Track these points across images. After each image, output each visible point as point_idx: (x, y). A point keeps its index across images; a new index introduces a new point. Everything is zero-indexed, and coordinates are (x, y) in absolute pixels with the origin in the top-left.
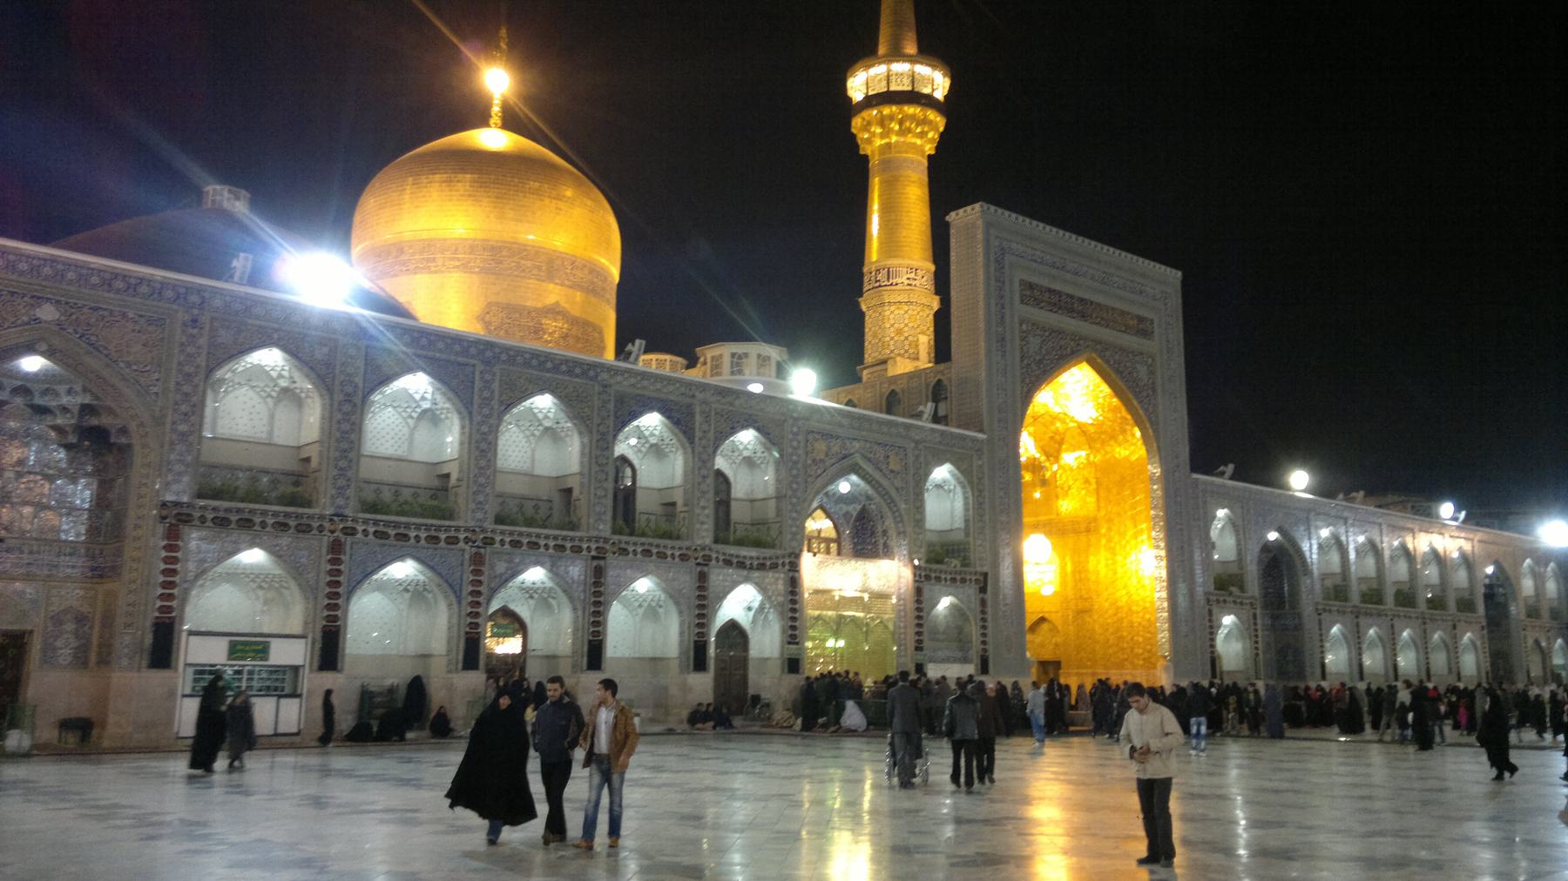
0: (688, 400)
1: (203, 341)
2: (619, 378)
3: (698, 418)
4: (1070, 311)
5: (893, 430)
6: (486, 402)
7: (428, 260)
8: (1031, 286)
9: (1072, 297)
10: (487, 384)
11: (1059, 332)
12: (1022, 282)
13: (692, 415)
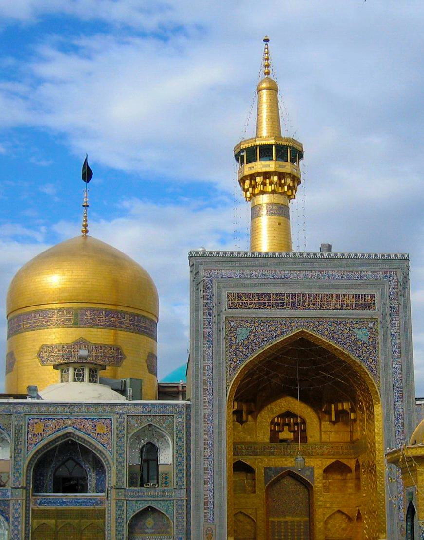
4: (281, 305)
5: (100, 409)
8: (239, 296)
9: (282, 295)
11: (268, 321)
12: (230, 295)
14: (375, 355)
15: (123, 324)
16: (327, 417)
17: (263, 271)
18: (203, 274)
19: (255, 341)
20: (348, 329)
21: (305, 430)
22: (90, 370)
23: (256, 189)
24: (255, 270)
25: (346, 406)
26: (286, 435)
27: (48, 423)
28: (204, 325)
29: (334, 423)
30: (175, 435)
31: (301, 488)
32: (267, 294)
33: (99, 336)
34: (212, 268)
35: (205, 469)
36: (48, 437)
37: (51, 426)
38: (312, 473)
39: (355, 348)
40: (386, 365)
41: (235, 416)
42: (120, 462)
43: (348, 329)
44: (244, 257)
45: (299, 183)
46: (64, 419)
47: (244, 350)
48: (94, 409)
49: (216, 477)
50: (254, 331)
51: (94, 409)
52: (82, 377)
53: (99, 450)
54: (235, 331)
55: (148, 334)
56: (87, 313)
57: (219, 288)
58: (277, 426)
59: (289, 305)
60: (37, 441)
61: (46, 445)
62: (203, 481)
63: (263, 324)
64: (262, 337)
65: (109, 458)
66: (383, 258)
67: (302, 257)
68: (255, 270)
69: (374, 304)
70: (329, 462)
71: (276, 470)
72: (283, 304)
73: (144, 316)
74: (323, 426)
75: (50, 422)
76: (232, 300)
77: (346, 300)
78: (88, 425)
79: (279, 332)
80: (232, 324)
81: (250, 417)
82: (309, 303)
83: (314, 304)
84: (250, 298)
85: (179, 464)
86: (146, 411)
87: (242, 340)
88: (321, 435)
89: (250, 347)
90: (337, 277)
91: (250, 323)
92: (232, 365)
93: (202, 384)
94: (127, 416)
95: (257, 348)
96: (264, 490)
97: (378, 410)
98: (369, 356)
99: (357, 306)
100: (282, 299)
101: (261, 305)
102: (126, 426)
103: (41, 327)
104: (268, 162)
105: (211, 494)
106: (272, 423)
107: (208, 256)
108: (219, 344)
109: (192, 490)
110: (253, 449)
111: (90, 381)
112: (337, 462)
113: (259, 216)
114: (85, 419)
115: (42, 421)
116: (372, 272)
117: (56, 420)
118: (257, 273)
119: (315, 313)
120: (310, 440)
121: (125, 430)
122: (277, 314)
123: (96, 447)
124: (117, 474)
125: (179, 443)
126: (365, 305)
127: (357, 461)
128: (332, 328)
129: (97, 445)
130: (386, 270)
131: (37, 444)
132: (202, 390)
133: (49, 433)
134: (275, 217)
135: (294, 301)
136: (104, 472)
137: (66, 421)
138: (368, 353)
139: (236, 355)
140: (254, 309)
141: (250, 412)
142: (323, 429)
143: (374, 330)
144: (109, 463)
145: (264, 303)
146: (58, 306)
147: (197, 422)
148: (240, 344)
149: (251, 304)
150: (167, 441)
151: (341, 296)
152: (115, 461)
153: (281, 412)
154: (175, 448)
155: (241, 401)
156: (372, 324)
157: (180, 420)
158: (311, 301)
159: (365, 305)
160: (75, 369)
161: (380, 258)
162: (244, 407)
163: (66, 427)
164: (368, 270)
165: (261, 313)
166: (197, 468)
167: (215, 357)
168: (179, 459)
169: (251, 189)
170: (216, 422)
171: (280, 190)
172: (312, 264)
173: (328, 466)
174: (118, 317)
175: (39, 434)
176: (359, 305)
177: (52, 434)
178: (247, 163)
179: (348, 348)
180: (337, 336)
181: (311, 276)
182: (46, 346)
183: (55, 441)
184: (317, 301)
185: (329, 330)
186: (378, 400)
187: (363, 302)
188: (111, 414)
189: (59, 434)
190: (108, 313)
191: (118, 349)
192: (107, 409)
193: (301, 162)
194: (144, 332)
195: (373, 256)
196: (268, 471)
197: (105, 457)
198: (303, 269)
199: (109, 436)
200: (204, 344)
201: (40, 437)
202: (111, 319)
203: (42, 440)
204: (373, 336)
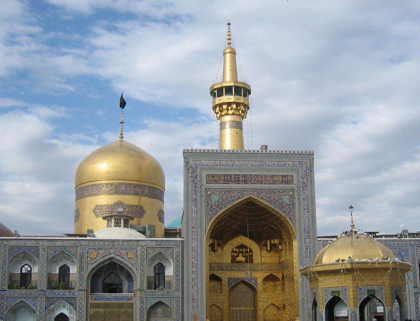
3: (41, 251)
4: (238, 182)
5: (130, 243)
8: (213, 176)
9: (238, 175)
11: (230, 191)
12: (207, 175)
13: (39, 250)
14: (293, 211)
15: (144, 193)
16: (265, 248)
17: (227, 161)
18: (191, 163)
19: (222, 202)
20: (277, 195)
21: (252, 256)
22: (124, 220)
23: (223, 113)
24: (222, 161)
25: (276, 241)
26: (241, 258)
27: (99, 252)
28: (192, 193)
29: (269, 251)
30: (175, 259)
31: (249, 290)
32: (229, 175)
33: (130, 200)
34: (196, 159)
35: (193, 279)
36: (99, 260)
37: (101, 253)
38: (256, 281)
39: (282, 207)
40: (300, 217)
41: (210, 247)
42: (142, 275)
43: (277, 195)
44: (216, 153)
45: (248, 109)
46: (109, 249)
47: (216, 208)
48: (127, 243)
49: (199, 284)
50: (222, 197)
51: (127, 243)
52: (119, 224)
53: (130, 267)
54: (210, 197)
55: (159, 198)
56: (122, 186)
57: (201, 171)
58: (235, 254)
59: (242, 181)
60: (93, 262)
61: (98, 265)
62: (191, 286)
63: (227, 193)
64: (227, 200)
65: (136, 273)
66: (298, 153)
67: (250, 153)
68: (222, 161)
69: (293, 181)
70: (266, 275)
71: (235, 279)
72: (239, 181)
73: (156, 188)
74: (262, 253)
75: (101, 251)
76: (208, 178)
77: (276, 179)
78: (123, 253)
79: (236, 198)
80: (209, 192)
81: (219, 248)
82: (254, 180)
83: (257, 181)
84: (219, 177)
85: (177, 275)
86: (157, 245)
87: (215, 202)
88: (261, 258)
89: (219, 206)
90: (271, 165)
91: (219, 192)
92: (209, 217)
93: (191, 228)
94: (146, 247)
95: (224, 207)
96: (228, 292)
97: (295, 243)
98: (290, 211)
99: (282, 182)
100: (239, 178)
101: (226, 182)
102: (145, 253)
103: (95, 195)
104: (230, 97)
105: (196, 293)
106: (232, 251)
107: (194, 152)
108: (201, 204)
109: (185, 291)
110: (221, 267)
111: (124, 227)
112: (271, 275)
113: (224, 128)
114: (121, 249)
115: (96, 250)
116: (291, 161)
117: (104, 249)
118: (223, 162)
119: (258, 186)
120: (254, 261)
121: (145, 255)
122: (235, 187)
123: (128, 266)
124: (140, 282)
125: (177, 264)
126: (288, 181)
127: (283, 274)
128: (268, 195)
129: (128, 264)
130: (300, 161)
131: (93, 264)
132: (191, 232)
133: (100, 257)
134: (234, 129)
135: (246, 179)
136: (133, 281)
137: (110, 250)
138: (289, 210)
139: (211, 211)
140: (222, 184)
141: (219, 245)
142: (263, 255)
143: (293, 196)
144: (135, 275)
145: (227, 180)
146: (106, 182)
147: (188, 251)
148: (213, 205)
149: (220, 181)
150: (170, 262)
151: (274, 176)
152: (139, 274)
153: (237, 245)
154: (175, 267)
155: (214, 238)
156: (292, 193)
157: (178, 250)
158: (256, 179)
159: (288, 181)
160: (115, 219)
161: (297, 153)
162: (216, 242)
163: (110, 254)
164: (289, 160)
165: (226, 186)
166: (188, 278)
167: (199, 212)
168: (178, 273)
169: (220, 112)
170: (199, 251)
171: (237, 113)
172: (256, 157)
173: (265, 277)
174: (141, 189)
175: (94, 258)
176: (284, 181)
177: (102, 258)
178: (217, 97)
179: (278, 207)
180: (271, 200)
181: (255, 164)
182: (99, 206)
183: (103, 262)
184: (259, 179)
185: (266, 196)
186: (295, 238)
187: (286, 180)
188: (137, 246)
189: (106, 258)
190: (135, 186)
191: (141, 207)
192: (135, 243)
193: (250, 96)
194: (157, 197)
195: (292, 152)
196: (230, 280)
197: (134, 272)
198: (251, 160)
199: (136, 259)
200: (192, 205)
201: (95, 260)
202: (137, 189)
203: (96, 261)
204: (292, 200)
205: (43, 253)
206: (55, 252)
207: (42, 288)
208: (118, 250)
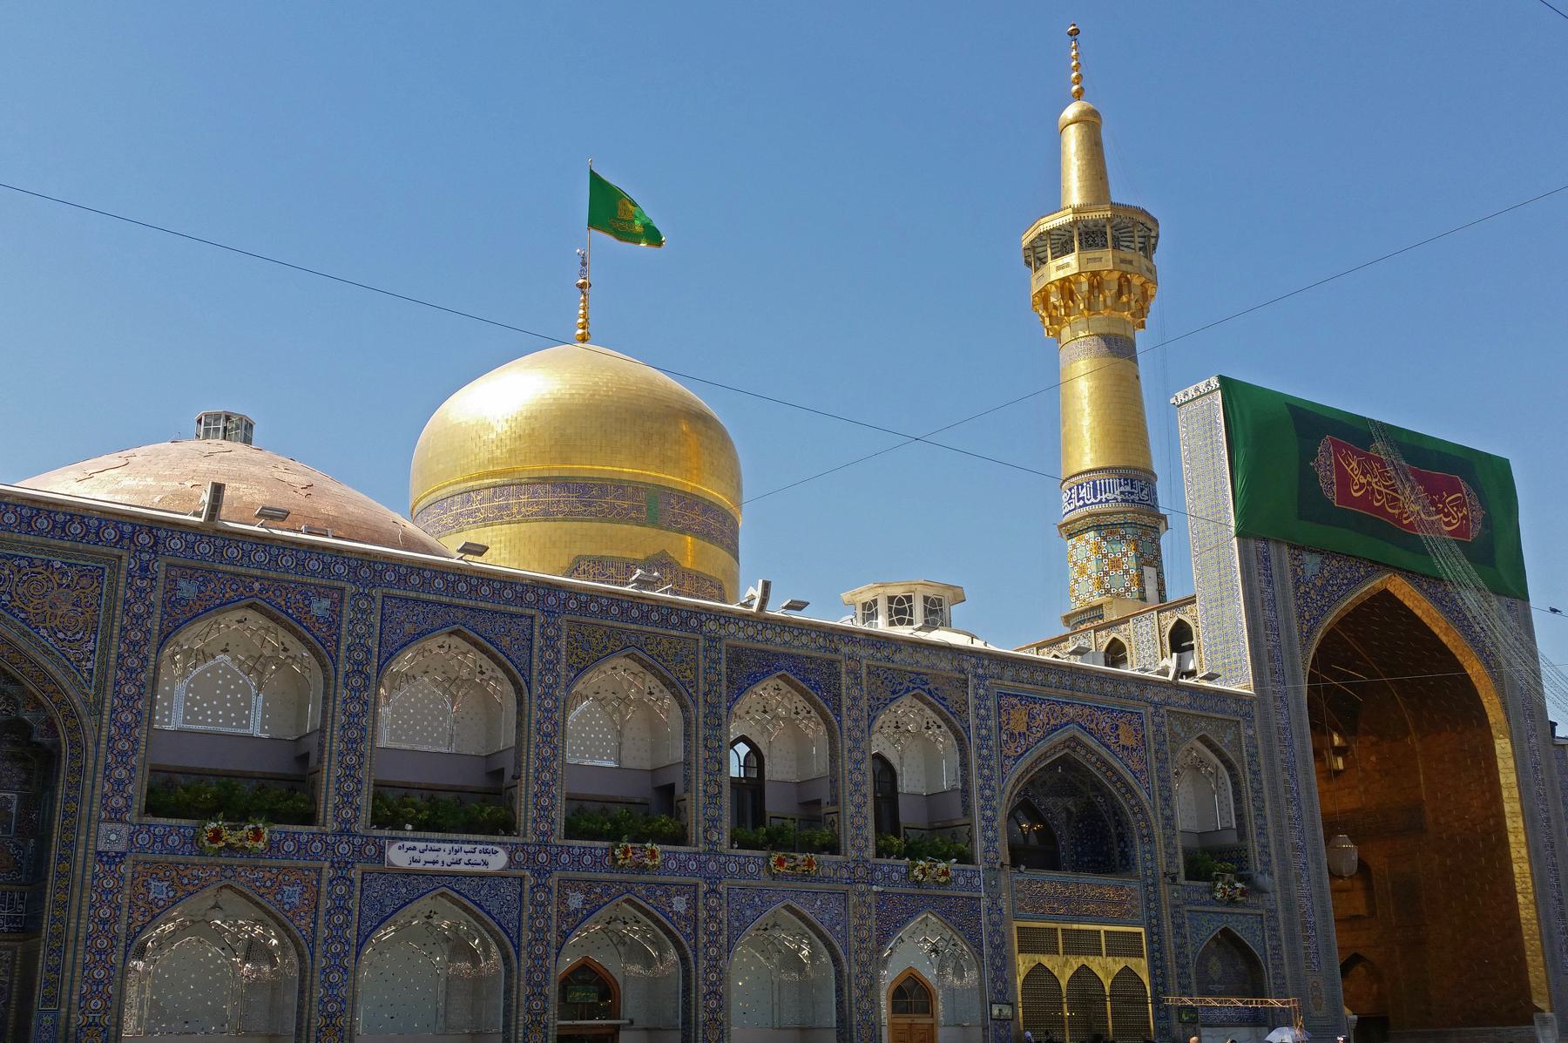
0: (833, 656)
1: (156, 597)
2: (732, 628)
3: (845, 680)
5: (1122, 690)
6: (549, 667)
7: (500, 508)
10: (550, 643)
13: (838, 675)
137: (1067, 709)
170: (1297, 744)
189: (1058, 737)
205: (855, 692)
206: (894, 692)
207: (860, 849)
208: (1087, 711)
